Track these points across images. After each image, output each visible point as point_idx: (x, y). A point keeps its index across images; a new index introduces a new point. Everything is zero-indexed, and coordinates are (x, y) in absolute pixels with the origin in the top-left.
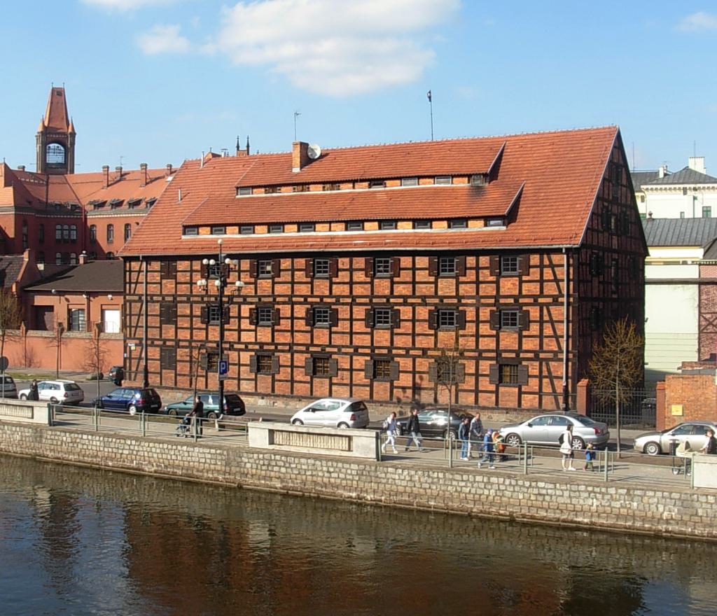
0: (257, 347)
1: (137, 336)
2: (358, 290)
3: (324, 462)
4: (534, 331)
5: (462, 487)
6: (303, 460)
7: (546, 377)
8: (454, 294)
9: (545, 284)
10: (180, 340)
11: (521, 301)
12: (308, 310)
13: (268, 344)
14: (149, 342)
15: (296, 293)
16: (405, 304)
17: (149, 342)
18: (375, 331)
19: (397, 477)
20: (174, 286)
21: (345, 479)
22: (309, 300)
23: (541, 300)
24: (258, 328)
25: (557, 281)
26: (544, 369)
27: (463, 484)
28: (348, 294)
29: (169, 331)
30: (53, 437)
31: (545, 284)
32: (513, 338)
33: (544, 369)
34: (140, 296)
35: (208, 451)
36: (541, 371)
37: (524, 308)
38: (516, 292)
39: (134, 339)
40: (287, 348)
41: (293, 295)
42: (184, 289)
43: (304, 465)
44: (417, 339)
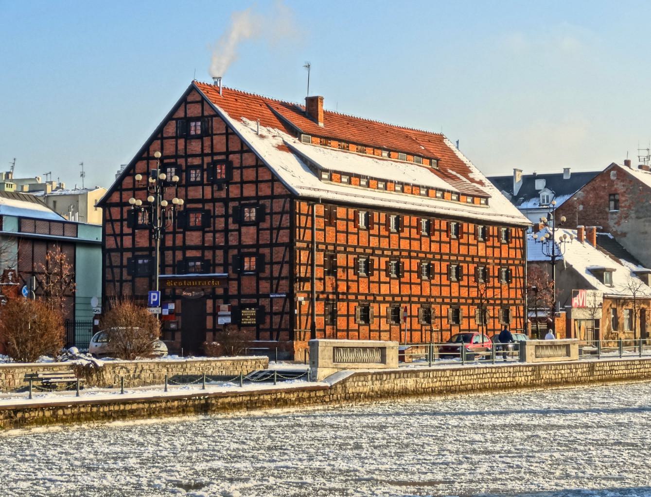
0: (390, 299)
1: (305, 289)
2: (445, 249)
24: (392, 281)
30: (600, 368)
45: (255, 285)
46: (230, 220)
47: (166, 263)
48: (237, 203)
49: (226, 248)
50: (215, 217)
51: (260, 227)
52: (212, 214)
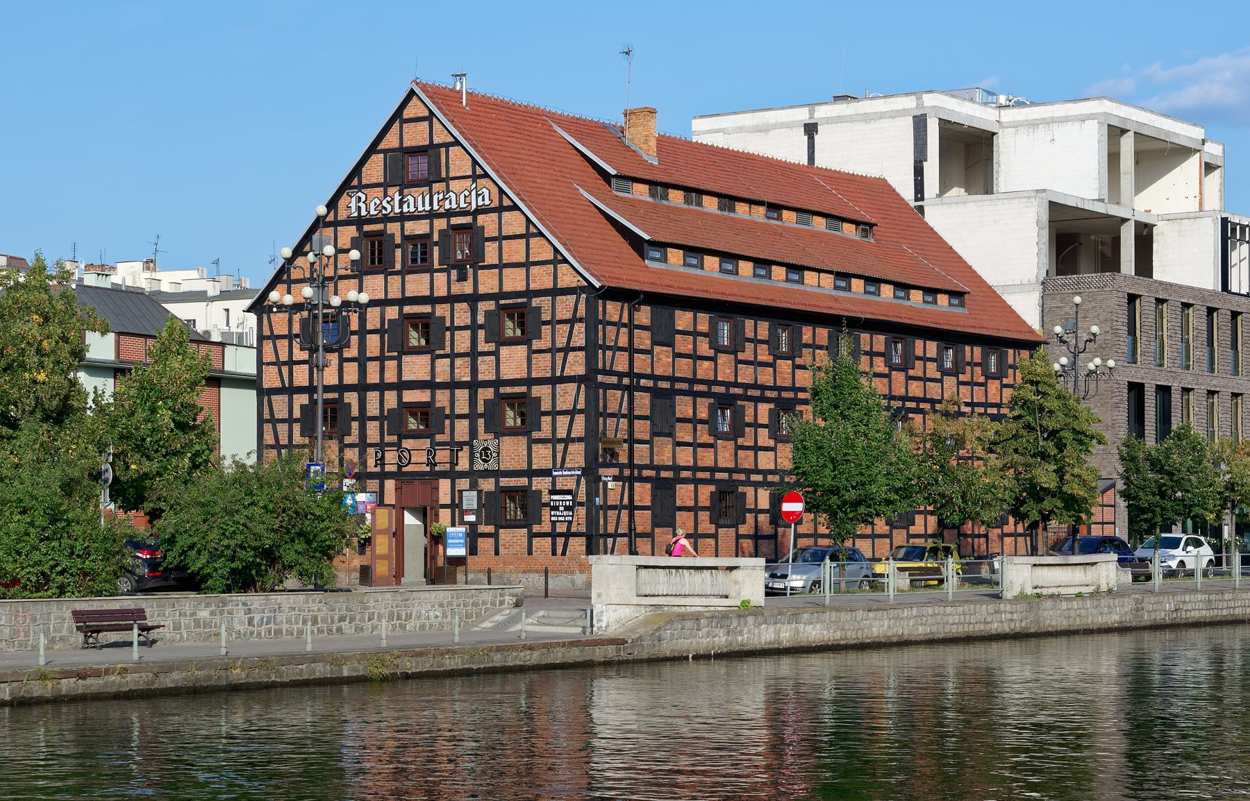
20: (671, 360)
45: (525, 453)
46: (481, 334)
47: (369, 414)
48: (493, 302)
49: (473, 386)
50: (453, 329)
51: (534, 347)
52: (448, 324)
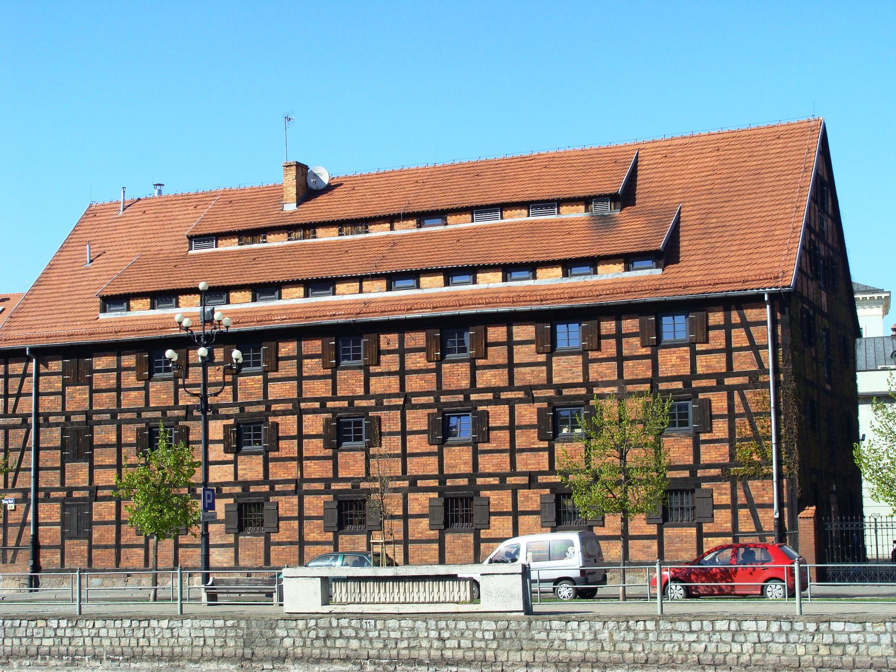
0: (238, 489)
2: (414, 383)
3: (432, 623)
4: (719, 431)
5: (690, 643)
6: (392, 623)
7: (743, 506)
8: (581, 380)
9: (735, 354)
10: (98, 488)
11: (695, 384)
12: (327, 422)
13: (257, 483)
14: (41, 495)
15: (307, 395)
16: (497, 401)
17: (41, 495)
18: (445, 450)
19: (568, 636)
21: (472, 648)
22: (330, 404)
23: (728, 381)
24: (240, 458)
25: (754, 348)
26: (740, 493)
27: (693, 637)
28: (398, 391)
29: (78, 474)
31: (735, 354)
32: (683, 446)
33: (740, 493)
34: (25, 417)
35: (209, 623)
36: (734, 498)
37: (701, 396)
38: (686, 371)
39: (14, 490)
40: (292, 487)
41: (300, 399)
42: (105, 401)
43: (394, 630)
44: (519, 457)
